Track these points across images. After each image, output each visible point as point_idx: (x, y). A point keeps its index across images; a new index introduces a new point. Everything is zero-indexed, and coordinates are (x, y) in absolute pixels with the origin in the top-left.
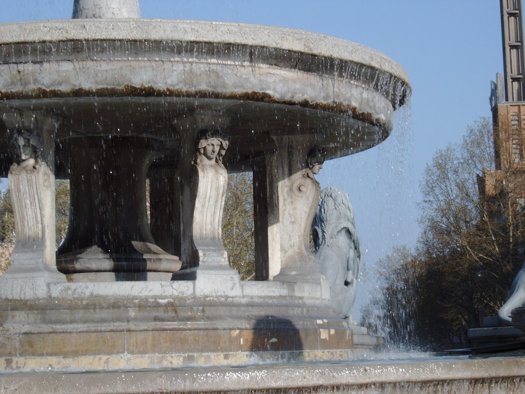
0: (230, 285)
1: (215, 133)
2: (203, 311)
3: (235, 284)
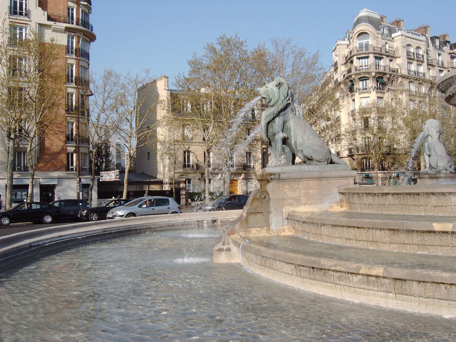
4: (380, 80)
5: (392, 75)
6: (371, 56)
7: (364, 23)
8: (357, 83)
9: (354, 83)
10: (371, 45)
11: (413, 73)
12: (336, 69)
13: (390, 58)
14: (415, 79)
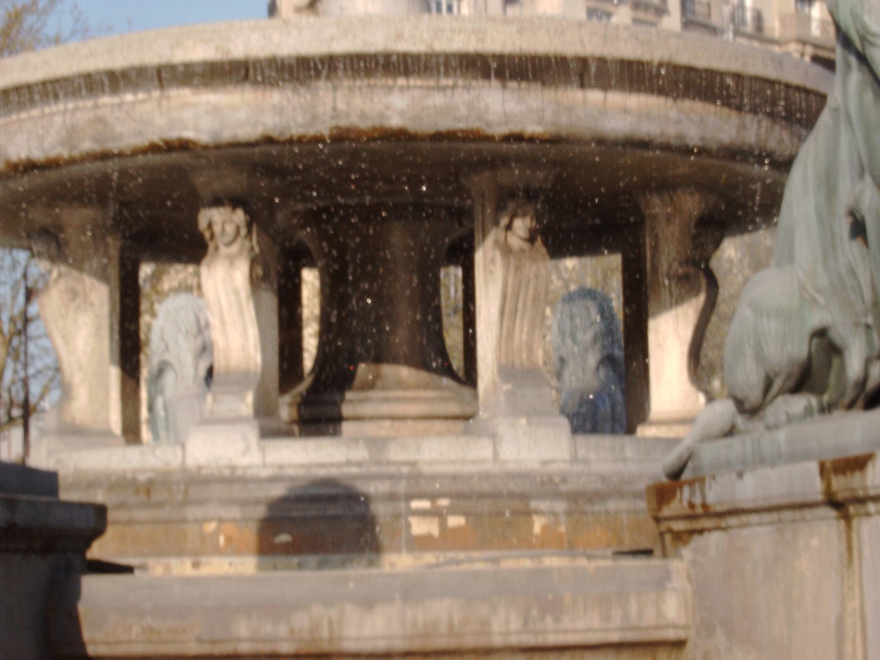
0: (241, 446)
1: (217, 202)
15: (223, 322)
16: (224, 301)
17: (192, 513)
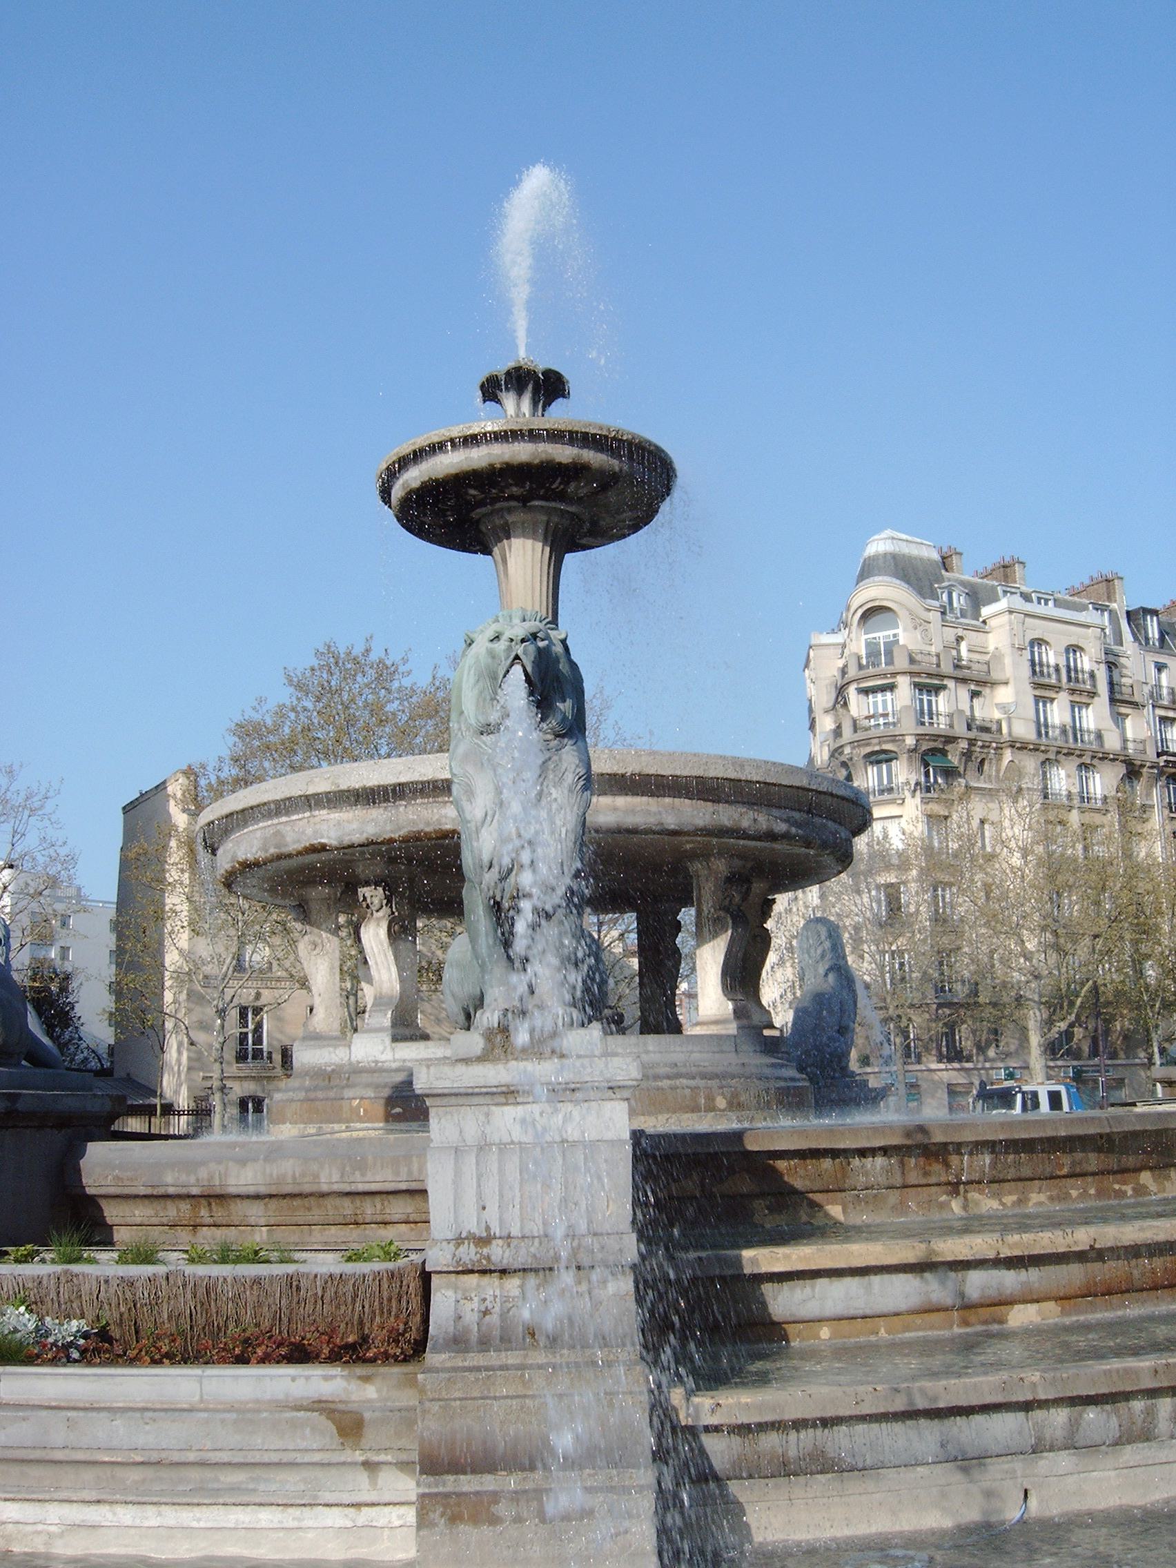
0: (381, 1048)
2: (349, 1078)
3: (385, 1047)
4: (934, 762)
5: (980, 743)
6: (904, 683)
7: (881, 578)
8: (861, 772)
9: (853, 772)
10: (904, 646)
11: (1057, 732)
12: (812, 726)
13: (973, 687)
14: (1065, 751)
15: (376, 963)
16: (376, 950)
17: (348, 1093)
